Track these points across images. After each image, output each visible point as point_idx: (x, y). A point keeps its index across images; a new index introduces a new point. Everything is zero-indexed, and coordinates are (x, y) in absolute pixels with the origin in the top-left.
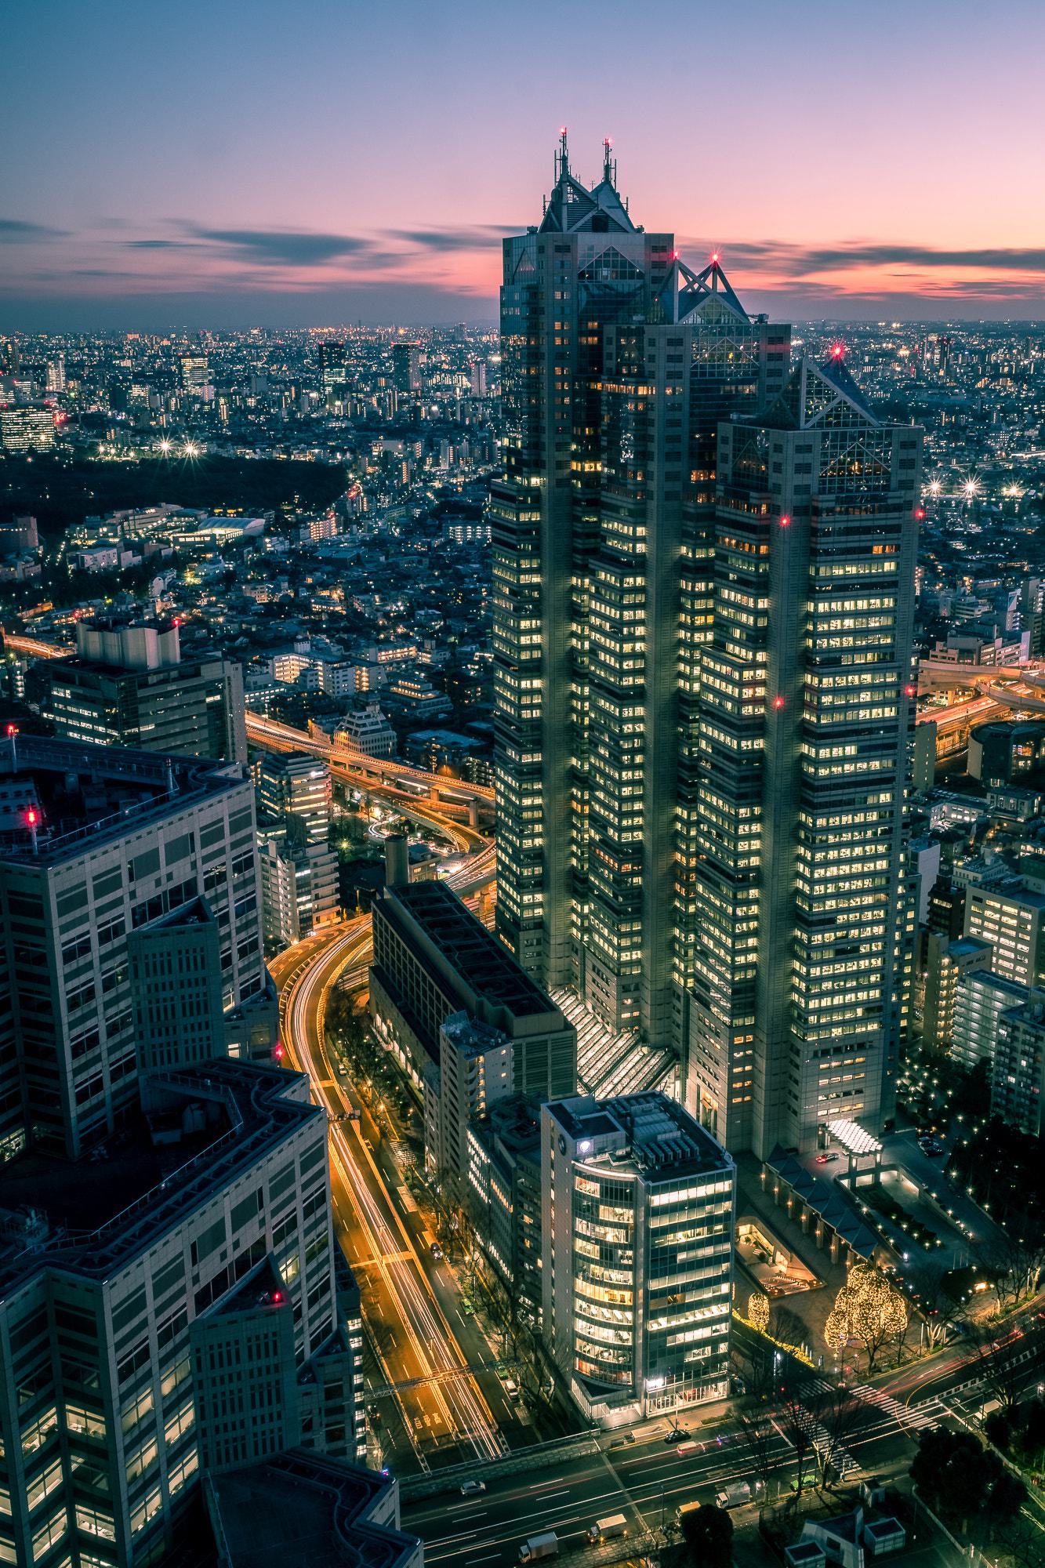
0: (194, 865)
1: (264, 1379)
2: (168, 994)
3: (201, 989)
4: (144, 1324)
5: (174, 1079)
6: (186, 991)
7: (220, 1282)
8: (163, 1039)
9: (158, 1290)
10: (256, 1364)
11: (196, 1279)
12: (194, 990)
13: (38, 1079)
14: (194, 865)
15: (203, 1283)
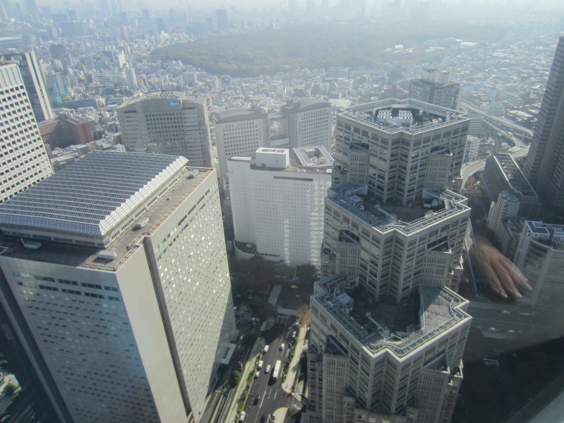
0: (449, 139)
1: (440, 268)
2: (435, 171)
3: (444, 171)
4: (415, 248)
5: (432, 192)
6: (440, 171)
7: (434, 243)
8: (431, 182)
9: (420, 240)
10: (439, 264)
11: (429, 241)
12: (442, 171)
13: (399, 185)
14: (449, 139)
15: (430, 242)
